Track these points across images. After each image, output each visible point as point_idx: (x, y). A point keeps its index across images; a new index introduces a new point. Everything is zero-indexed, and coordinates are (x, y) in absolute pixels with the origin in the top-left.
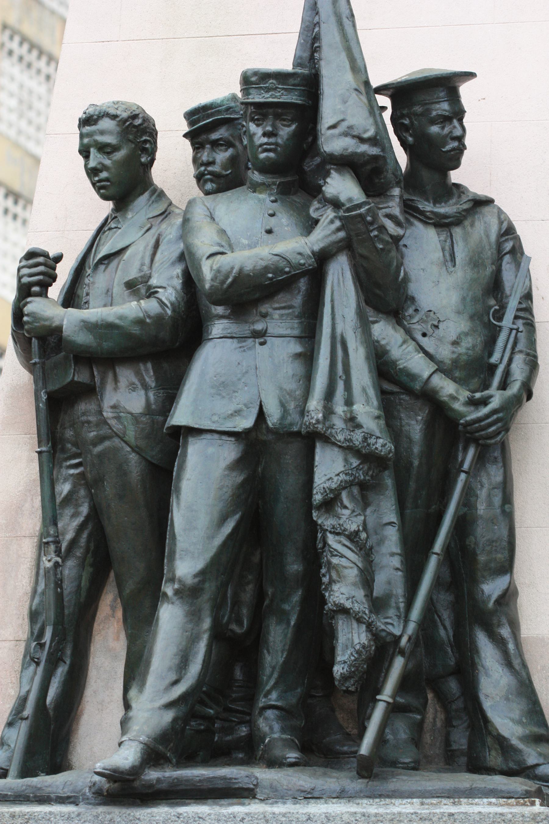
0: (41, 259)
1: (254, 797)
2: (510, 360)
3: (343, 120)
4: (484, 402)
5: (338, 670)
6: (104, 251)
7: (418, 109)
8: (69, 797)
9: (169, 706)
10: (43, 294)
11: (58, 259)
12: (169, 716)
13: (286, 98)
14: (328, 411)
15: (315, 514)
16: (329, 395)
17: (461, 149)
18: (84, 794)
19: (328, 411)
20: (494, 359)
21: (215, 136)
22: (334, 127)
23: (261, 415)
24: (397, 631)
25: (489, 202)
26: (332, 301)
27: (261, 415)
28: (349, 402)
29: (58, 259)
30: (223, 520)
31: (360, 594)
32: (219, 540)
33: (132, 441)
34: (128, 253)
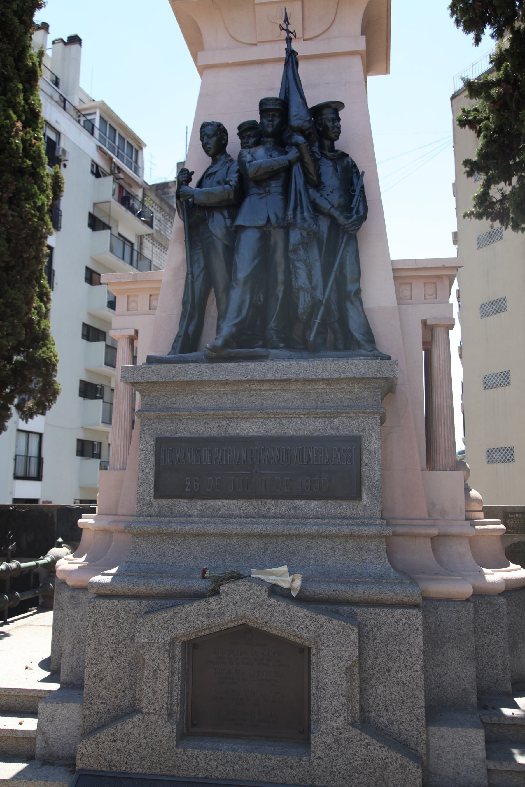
0: (186, 172)
1: (268, 359)
2: (359, 206)
3: (298, 114)
4: (351, 217)
5: (300, 311)
6: (210, 172)
7: (324, 117)
8: (196, 360)
9: (235, 325)
10: (187, 184)
11: (193, 173)
12: (234, 330)
13: (277, 107)
14: (295, 216)
15: (290, 255)
16: (295, 210)
17: (339, 132)
18: (202, 359)
19: (295, 216)
20: (353, 206)
21: (248, 133)
22: (295, 116)
23: (268, 220)
24: (321, 299)
25: (347, 155)
26: (295, 178)
27: (268, 220)
28: (302, 213)
29: (193, 173)
30: (254, 258)
31: (307, 283)
32: (253, 265)
33: (220, 237)
34: (217, 173)
